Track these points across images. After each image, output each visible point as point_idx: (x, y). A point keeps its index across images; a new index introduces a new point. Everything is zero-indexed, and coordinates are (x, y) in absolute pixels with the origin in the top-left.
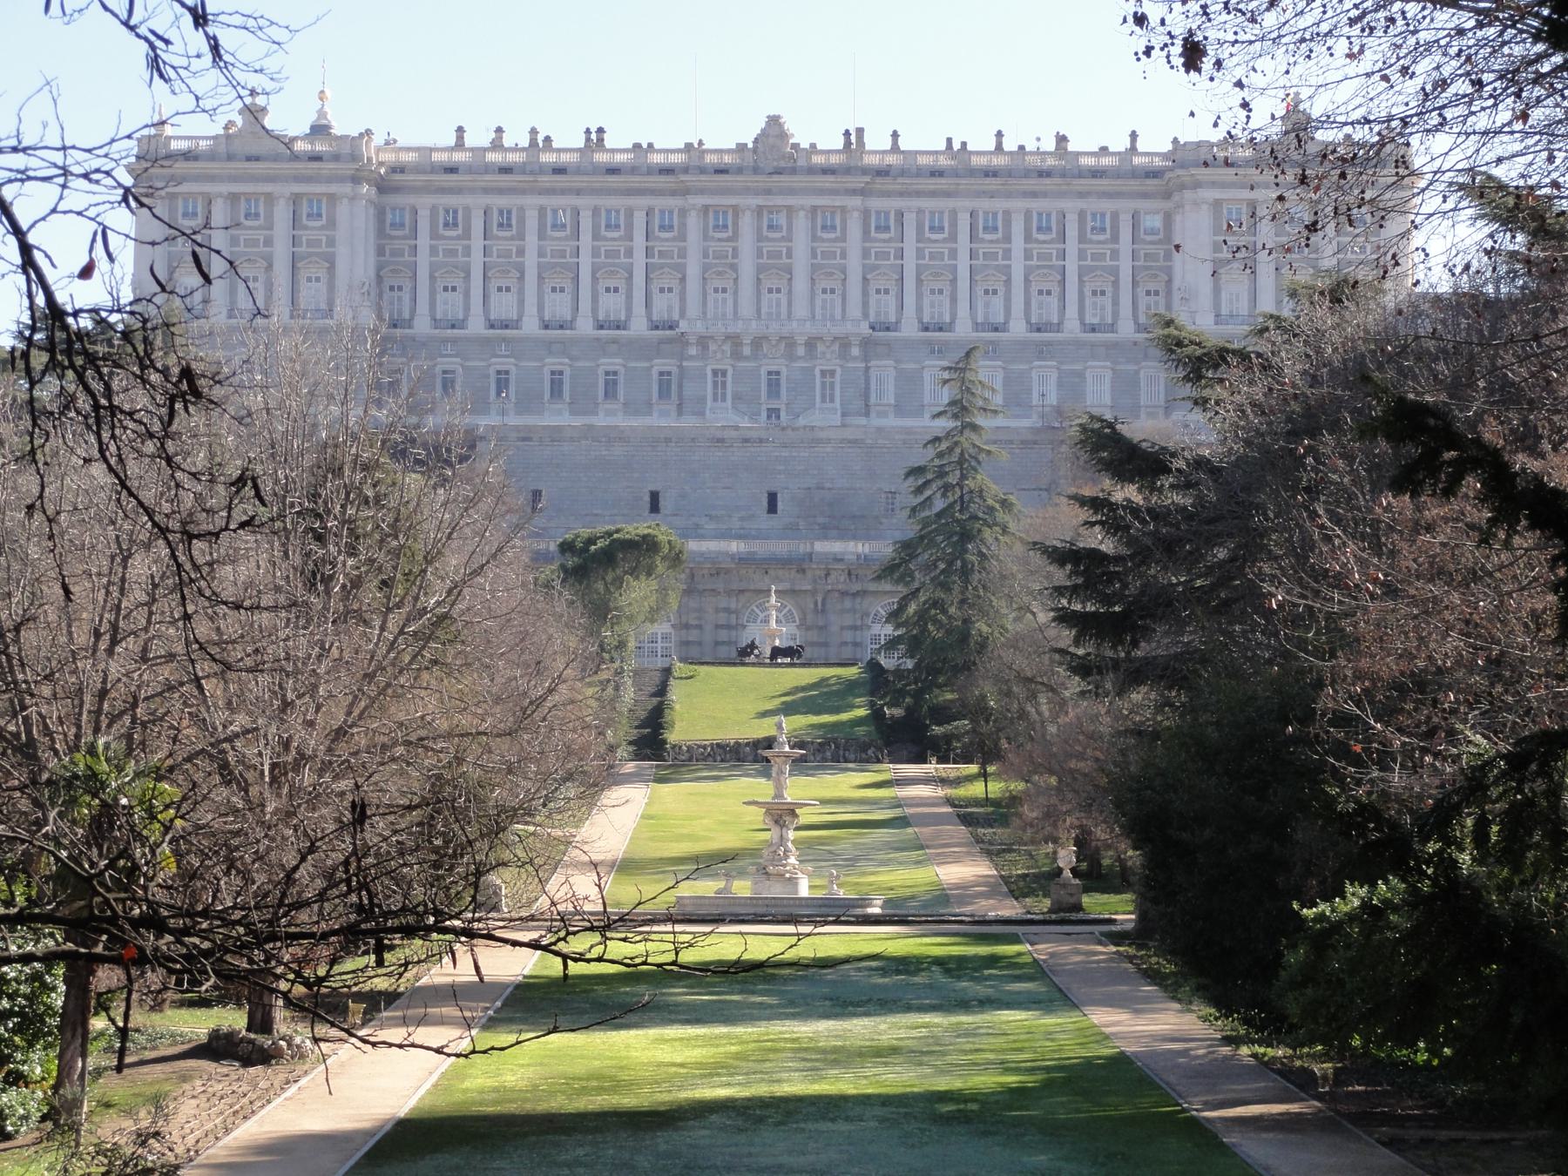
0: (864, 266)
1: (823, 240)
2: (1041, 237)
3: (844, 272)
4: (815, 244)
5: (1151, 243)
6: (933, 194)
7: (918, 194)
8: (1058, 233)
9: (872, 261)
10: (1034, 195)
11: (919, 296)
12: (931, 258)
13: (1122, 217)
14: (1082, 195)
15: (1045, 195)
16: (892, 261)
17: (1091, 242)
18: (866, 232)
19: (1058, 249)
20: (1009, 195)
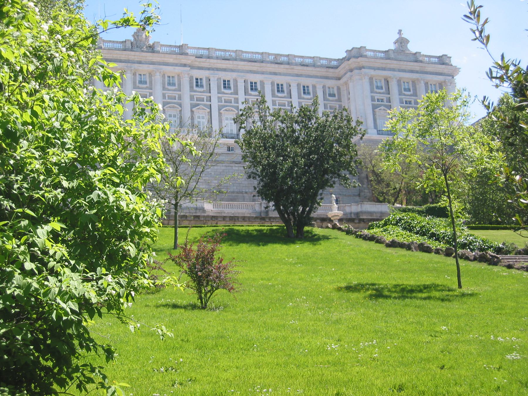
0: (191, 104)
1: (169, 90)
2: (280, 95)
3: (180, 105)
4: (164, 92)
5: (332, 101)
6: (225, 70)
7: (218, 69)
8: (287, 93)
9: (195, 102)
10: (275, 74)
11: (220, 121)
12: (225, 102)
13: (318, 86)
14: (298, 75)
15: (280, 74)
16: (205, 102)
17: (304, 99)
18: (191, 87)
19: (288, 102)
20: (263, 73)
